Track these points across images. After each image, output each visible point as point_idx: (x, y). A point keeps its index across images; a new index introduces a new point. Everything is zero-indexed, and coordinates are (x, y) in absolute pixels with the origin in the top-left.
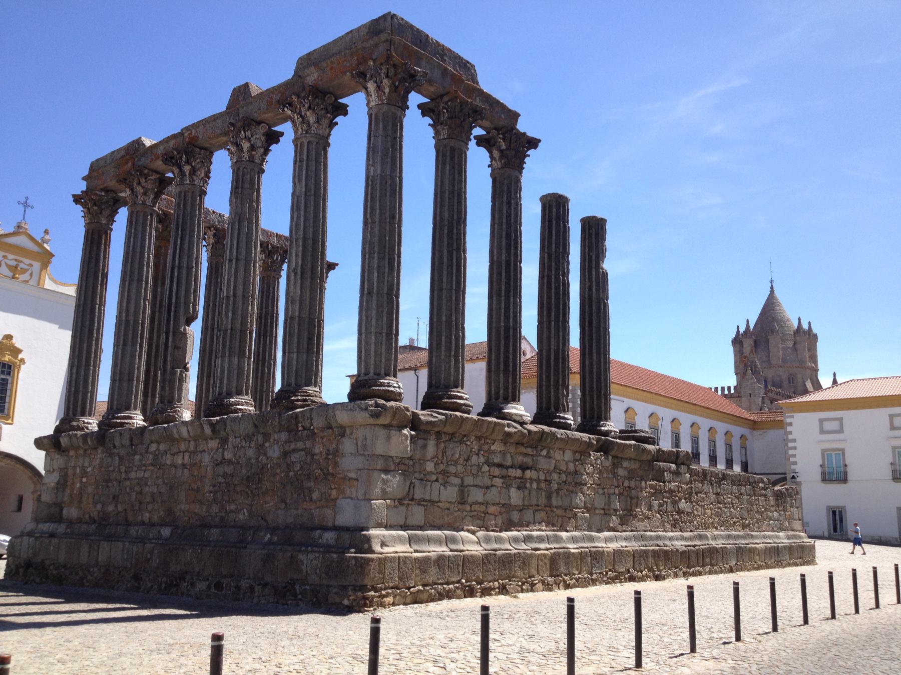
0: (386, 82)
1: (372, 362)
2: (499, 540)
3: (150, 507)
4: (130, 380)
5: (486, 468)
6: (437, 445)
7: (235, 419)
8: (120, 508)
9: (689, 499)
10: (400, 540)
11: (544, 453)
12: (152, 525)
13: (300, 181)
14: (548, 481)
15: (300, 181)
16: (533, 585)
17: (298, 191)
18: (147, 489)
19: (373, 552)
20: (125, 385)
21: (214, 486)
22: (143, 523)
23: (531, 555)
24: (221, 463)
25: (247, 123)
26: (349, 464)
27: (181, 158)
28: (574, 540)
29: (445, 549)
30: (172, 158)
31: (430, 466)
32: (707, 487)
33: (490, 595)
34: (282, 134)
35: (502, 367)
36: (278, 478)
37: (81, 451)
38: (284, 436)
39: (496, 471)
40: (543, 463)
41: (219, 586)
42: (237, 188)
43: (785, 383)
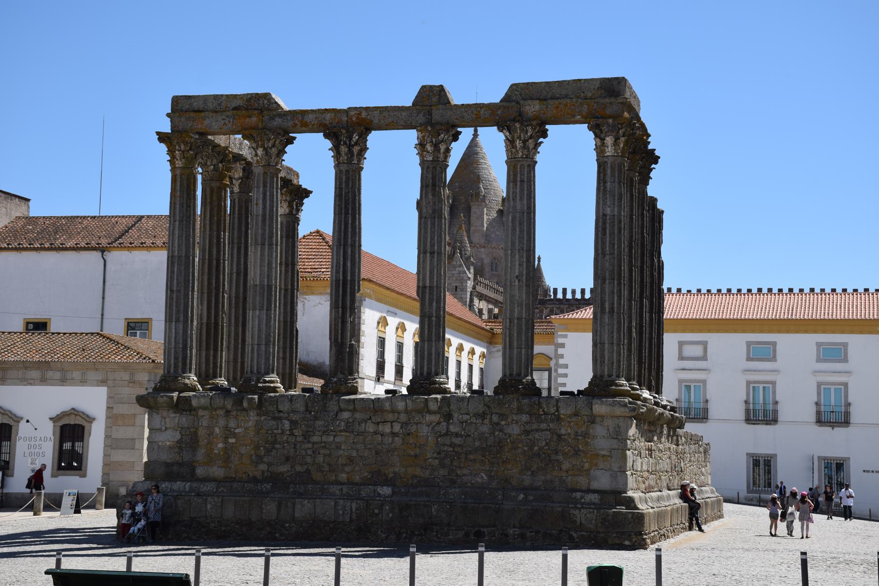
3: (348, 469)
12: (350, 483)
15: (521, 199)
17: (518, 207)
18: (342, 452)
21: (439, 453)
24: (446, 434)
27: (351, 139)
36: (519, 451)
37: (221, 412)
38: (525, 418)
42: (434, 185)
43: (487, 269)
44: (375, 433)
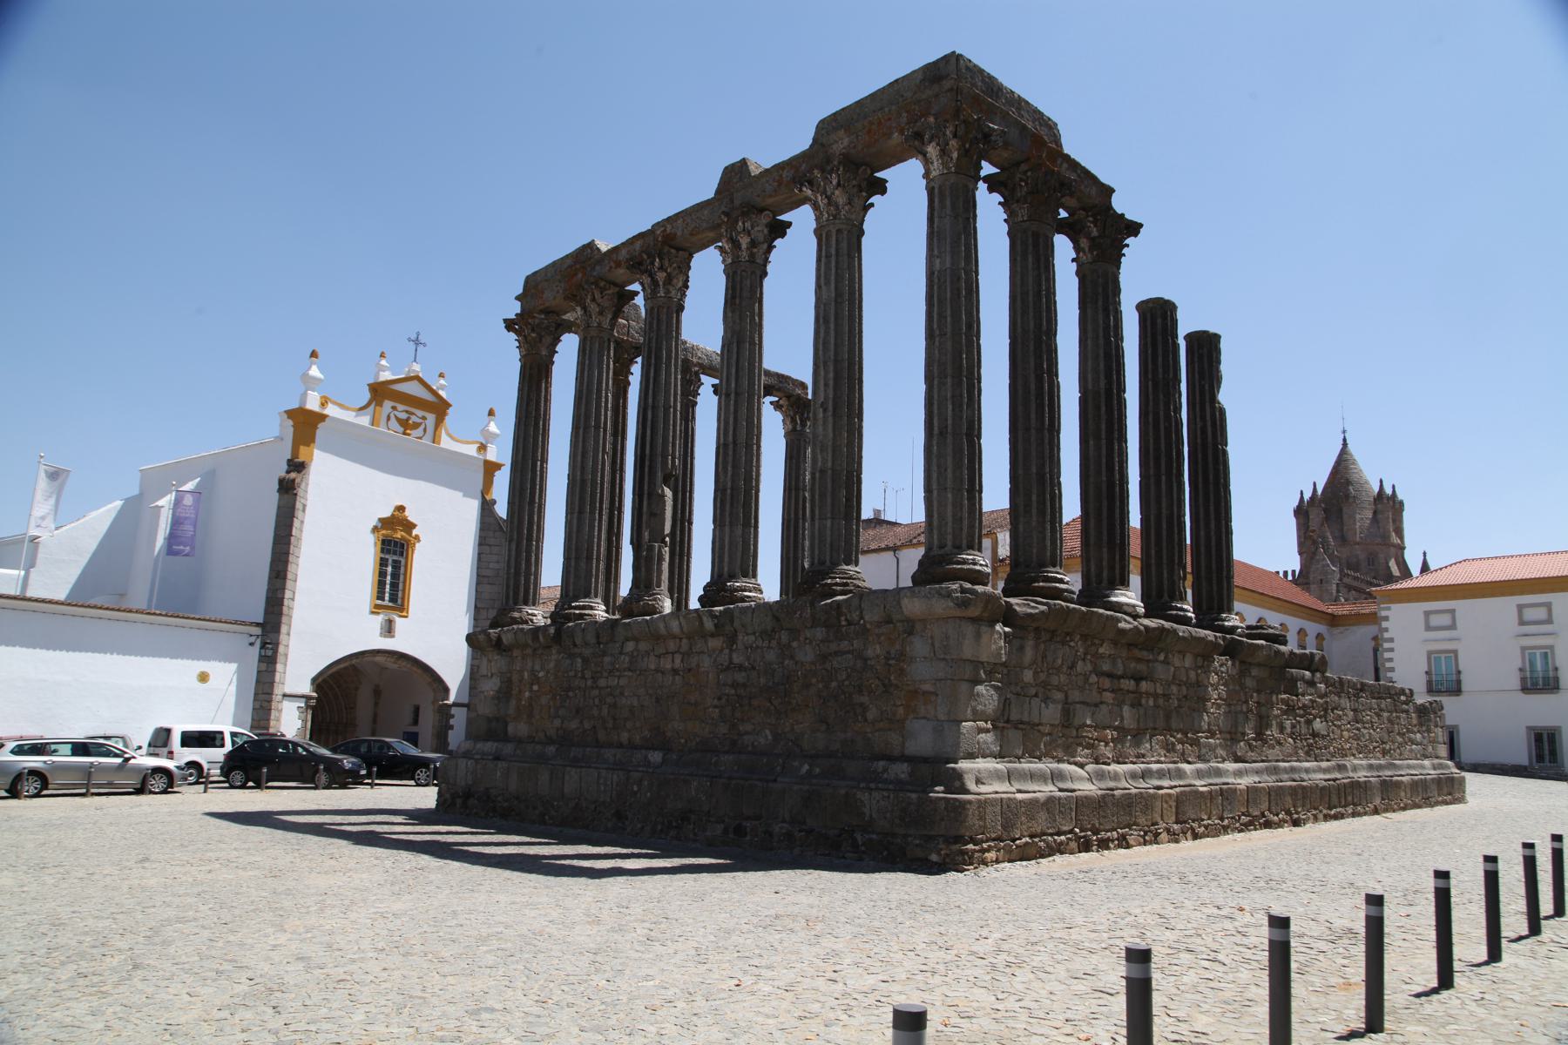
0: (953, 143)
1: (950, 530)
2: (1116, 777)
3: (629, 724)
4: (589, 558)
5: (1093, 679)
6: (1036, 647)
7: (744, 611)
8: (587, 725)
9: (1324, 718)
10: (997, 776)
11: (1162, 657)
13: (827, 283)
14: (1167, 696)
15: (827, 283)
16: (1157, 835)
19: (967, 792)
20: (583, 565)
22: (621, 746)
23: (1154, 796)
24: (728, 668)
25: (743, 211)
26: (922, 671)
27: (652, 263)
28: (1199, 774)
29: (1052, 788)
30: (640, 264)
31: (1028, 676)
32: (1345, 702)
33: (1108, 848)
34: (789, 224)
35: (1105, 538)
37: (529, 651)
38: (820, 633)
39: (1107, 683)
40: (1161, 672)
41: (739, 831)
42: (733, 297)
44: (657, 671)
